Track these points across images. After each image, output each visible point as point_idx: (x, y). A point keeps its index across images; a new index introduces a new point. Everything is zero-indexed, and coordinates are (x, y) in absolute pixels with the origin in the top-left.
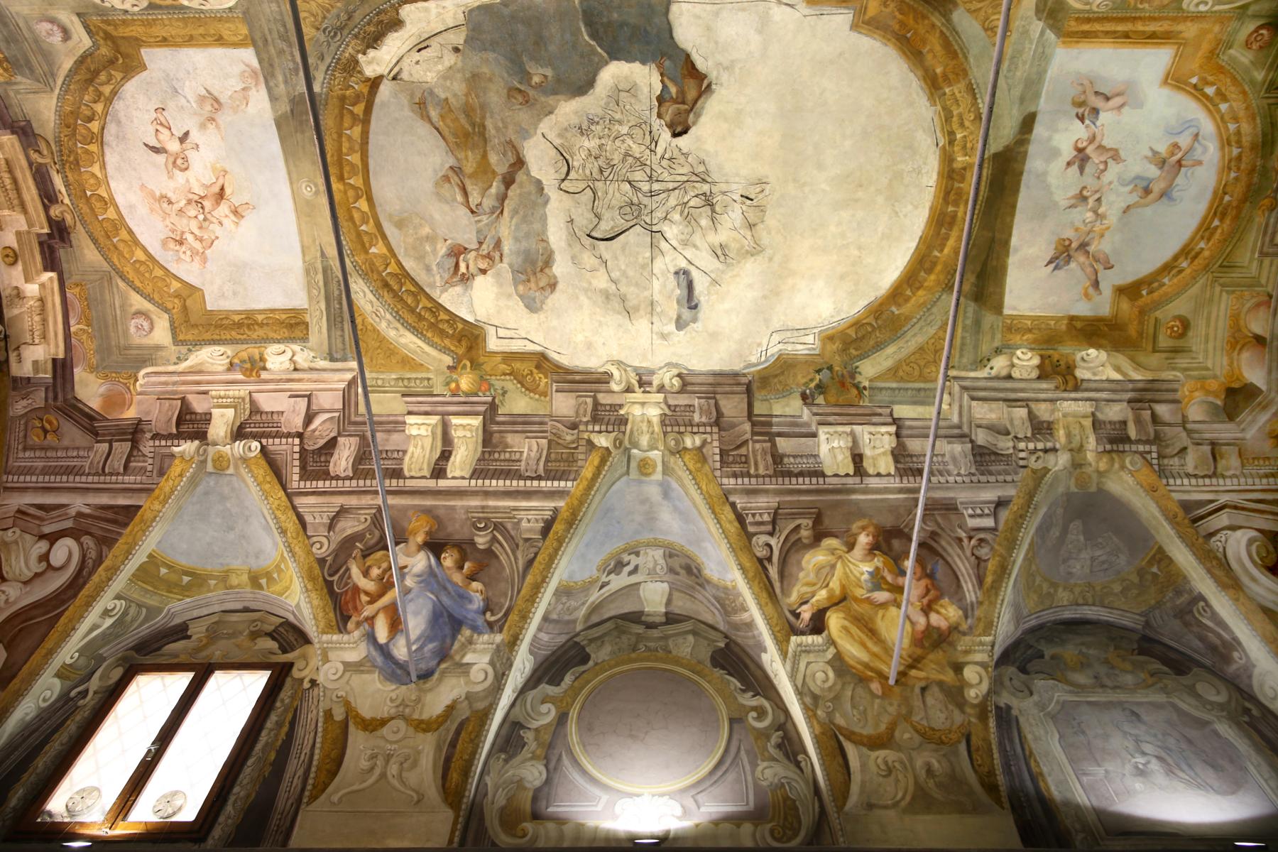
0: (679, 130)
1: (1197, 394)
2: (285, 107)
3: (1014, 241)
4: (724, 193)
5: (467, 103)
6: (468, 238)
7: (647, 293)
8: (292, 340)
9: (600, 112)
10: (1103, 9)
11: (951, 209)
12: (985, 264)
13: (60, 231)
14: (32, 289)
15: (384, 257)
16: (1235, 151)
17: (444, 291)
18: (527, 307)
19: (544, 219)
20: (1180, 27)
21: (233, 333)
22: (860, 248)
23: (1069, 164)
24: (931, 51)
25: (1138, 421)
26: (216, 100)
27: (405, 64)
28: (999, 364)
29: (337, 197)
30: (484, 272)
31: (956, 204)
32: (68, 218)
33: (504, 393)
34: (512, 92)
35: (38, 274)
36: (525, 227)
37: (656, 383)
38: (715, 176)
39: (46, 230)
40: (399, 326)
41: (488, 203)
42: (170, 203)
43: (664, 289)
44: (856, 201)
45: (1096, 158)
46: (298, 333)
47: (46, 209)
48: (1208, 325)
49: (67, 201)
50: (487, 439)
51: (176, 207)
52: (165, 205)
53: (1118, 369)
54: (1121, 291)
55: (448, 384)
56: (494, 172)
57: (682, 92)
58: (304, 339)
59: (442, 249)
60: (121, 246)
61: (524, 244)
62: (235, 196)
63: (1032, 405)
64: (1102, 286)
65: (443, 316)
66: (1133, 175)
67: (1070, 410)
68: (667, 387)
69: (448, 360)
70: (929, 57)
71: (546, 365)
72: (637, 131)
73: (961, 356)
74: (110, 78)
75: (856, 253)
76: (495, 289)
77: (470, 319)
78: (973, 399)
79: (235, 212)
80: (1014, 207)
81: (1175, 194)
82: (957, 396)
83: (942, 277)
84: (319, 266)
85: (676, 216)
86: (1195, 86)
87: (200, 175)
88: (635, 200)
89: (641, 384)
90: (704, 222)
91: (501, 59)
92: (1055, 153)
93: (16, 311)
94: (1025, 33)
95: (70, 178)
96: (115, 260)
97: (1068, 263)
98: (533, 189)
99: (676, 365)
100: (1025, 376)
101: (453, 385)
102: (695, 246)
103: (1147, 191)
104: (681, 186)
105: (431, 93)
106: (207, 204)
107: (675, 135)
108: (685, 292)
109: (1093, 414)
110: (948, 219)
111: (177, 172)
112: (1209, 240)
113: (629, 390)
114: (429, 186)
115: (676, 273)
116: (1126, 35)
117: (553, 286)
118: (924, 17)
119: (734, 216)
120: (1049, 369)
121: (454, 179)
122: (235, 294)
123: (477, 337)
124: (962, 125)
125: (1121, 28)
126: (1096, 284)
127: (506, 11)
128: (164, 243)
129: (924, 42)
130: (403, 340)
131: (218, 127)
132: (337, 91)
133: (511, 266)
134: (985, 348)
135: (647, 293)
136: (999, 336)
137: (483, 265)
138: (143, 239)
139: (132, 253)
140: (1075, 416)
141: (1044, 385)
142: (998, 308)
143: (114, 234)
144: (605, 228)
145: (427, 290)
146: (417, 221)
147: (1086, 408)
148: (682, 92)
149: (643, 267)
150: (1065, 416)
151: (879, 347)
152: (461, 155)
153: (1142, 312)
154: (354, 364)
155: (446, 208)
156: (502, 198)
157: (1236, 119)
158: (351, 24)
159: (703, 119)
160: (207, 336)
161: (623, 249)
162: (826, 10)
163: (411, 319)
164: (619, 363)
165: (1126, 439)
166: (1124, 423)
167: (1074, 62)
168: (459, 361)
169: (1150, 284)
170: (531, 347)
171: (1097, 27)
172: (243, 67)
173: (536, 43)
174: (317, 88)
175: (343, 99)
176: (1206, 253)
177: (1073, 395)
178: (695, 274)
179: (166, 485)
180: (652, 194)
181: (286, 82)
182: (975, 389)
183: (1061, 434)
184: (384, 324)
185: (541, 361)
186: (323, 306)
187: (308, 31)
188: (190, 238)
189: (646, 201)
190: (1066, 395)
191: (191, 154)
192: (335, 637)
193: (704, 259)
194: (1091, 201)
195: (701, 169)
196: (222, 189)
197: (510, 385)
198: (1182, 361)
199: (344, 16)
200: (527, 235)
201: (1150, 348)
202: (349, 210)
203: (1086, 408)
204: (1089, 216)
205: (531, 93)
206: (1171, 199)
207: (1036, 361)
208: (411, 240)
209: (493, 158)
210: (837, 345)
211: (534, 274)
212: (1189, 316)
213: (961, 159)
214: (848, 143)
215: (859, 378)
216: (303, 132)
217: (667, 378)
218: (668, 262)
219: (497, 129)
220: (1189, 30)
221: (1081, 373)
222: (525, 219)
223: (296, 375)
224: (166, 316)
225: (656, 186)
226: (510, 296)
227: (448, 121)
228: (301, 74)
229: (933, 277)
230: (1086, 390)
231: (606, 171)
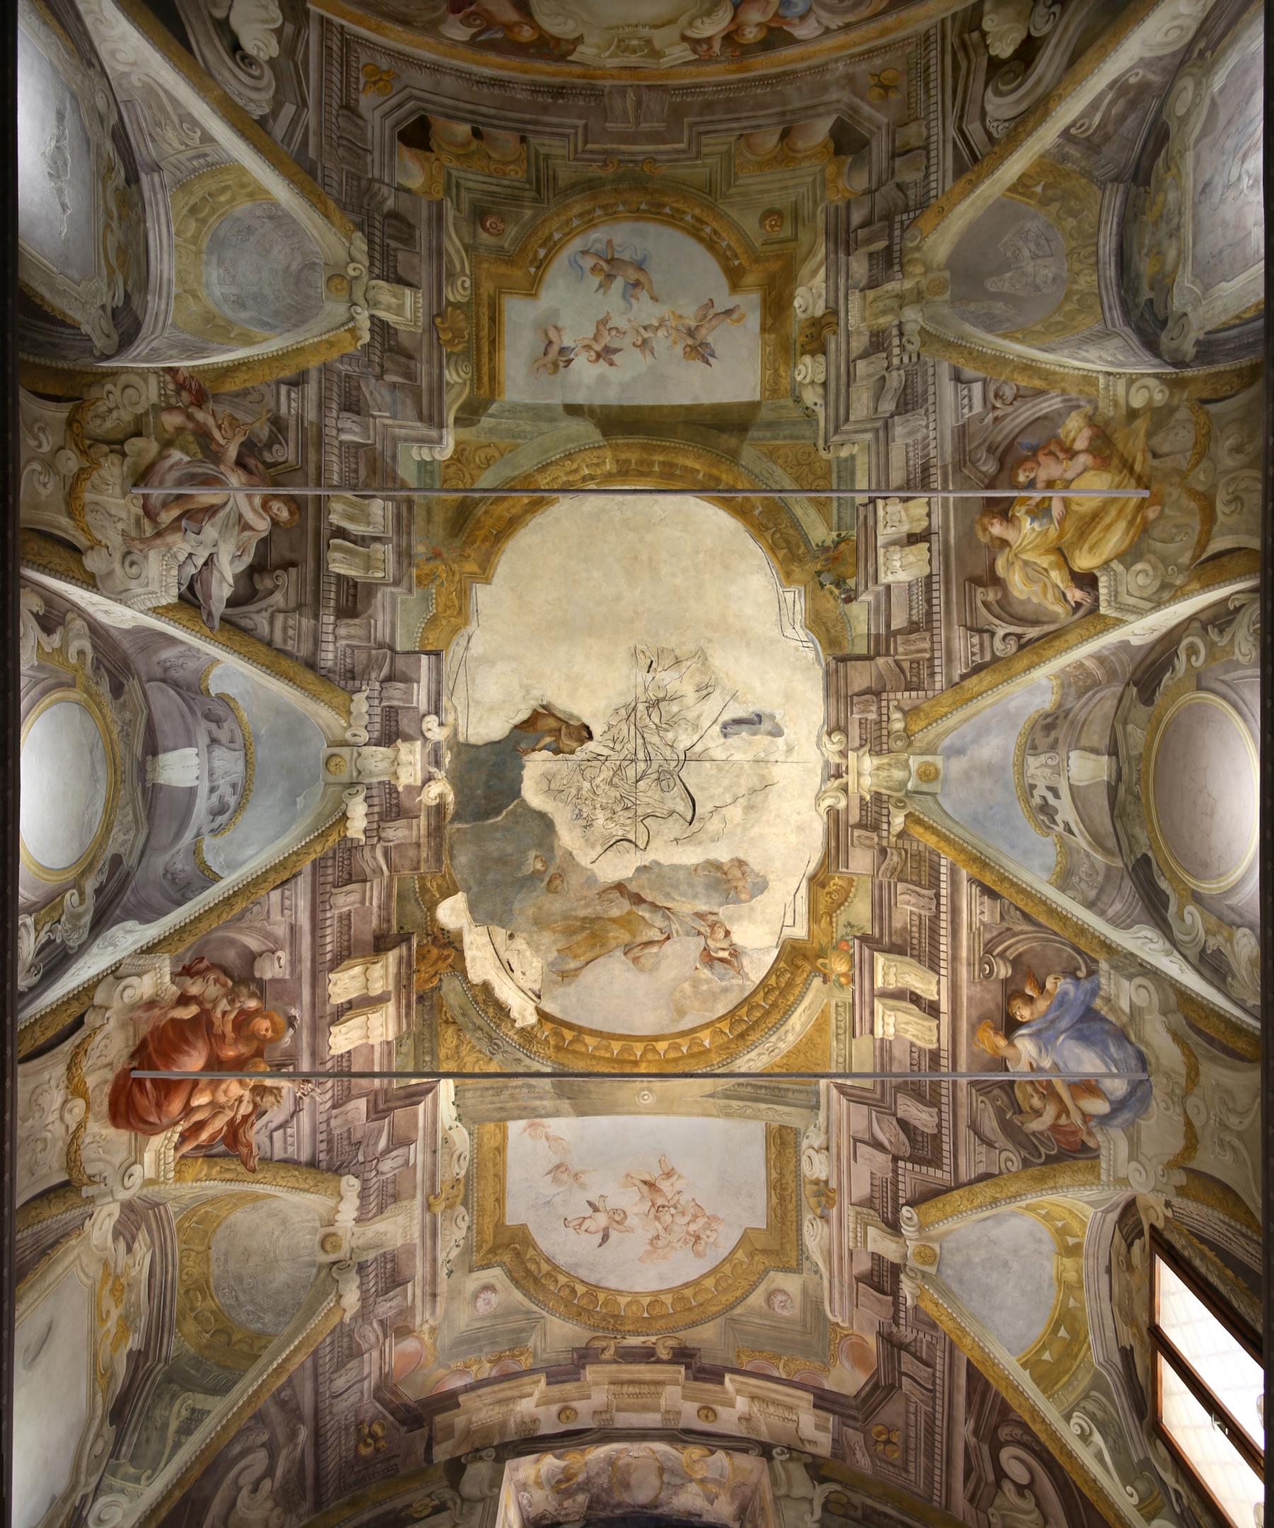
0: (585, 733)
1: (840, 186)
2: (565, 1104)
3: (687, 401)
4: (646, 689)
5: (562, 932)
6: (694, 946)
7: (746, 766)
8: (797, 1146)
9: (570, 808)
10: (469, 369)
11: (656, 468)
12: (710, 427)
13: (683, 1355)
15: (714, 1034)
16: (599, 212)
17: (746, 976)
18: (762, 892)
19: (675, 868)
20: (485, 297)
21: (790, 1207)
22: (697, 552)
23: (611, 364)
24: (508, 510)
25: (869, 241)
26: (558, 1167)
27: (527, 985)
28: (811, 397)
29: (654, 1070)
30: (727, 933)
31: (651, 464)
32: (670, 1343)
33: (850, 925)
34: (551, 888)
35: (726, 1392)
36: (683, 887)
37: (836, 759)
38: (630, 698)
39: (683, 1369)
40: (783, 1029)
41: (659, 921)
42: (657, 1237)
43: (742, 749)
44: (651, 560)
45: (606, 340)
46: (790, 1138)
47: (659, 1361)
48: (769, 191)
49: (653, 1339)
50: (898, 949)
51: (662, 1232)
52: (660, 1243)
53: (814, 273)
54: (735, 286)
55: (841, 986)
56: (629, 913)
57: (550, 732)
58: (796, 1132)
59: (705, 973)
60: (700, 1299)
61: (700, 889)
62: (654, 1174)
63: (853, 355)
64: (729, 306)
65: (773, 981)
66: (621, 302)
67: (856, 316)
68: (841, 747)
69: (817, 982)
70: (513, 511)
71: (821, 877)
72: (588, 773)
73: (803, 437)
74: (532, 1260)
75: (701, 556)
76: (746, 923)
77: (775, 953)
78: (847, 420)
79: (669, 1175)
80: (653, 408)
81: (639, 257)
82: (845, 437)
83: (724, 467)
84: (723, 1102)
85: (670, 736)
86: (538, 268)
87: (632, 1202)
88: (655, 776)
89: (838, 776)
90: (675, 708)
91: (520, 896)
92: (602, 380)
93: (764, 1428)
94: (491, 431)
95: (630, 1328)
96: (715, 1309)
97: (707, 345)
98: (645, 877)
99: (819, 737)
100: (823, 368)
101: (843, 980)
102: (699, 717)
103: (637, 284)
104: (640, 731)
105: (552, 964)
106: (660, 1201)
107: (590, 737)
108: (744, 727)
109: (862, 290)
110: (667, 470)
111: (627, 1223)
112: (684, 212)
113: (845, 789)
114: (643, 978)
115: (725, 736)
116: (492, 342)
117: (741, 863)
118: (478, 521)
119: (669, 679)
120: (815, 345)
121: (636, 952)
122: (750, 1196)
123: (793, 948)
124: (576, 471)
125: (486, 350)
126: (728, 313)
127: (475, 889)
128: (699, 1255)
129: (500, 518)
130: (798, 1028)
131: (584, 1172)
132: (551, 1052)
133: (721, 905)
134: (796, 414)
135: (746, 766)
136: (782, 402)
137: (722, 934)
138: (694, 1276)
139: (707, 1290)
140: (864, 309)
141: (832, 346)
142: (754, 406)
143: (686, 1302)
144: (682, 807)
145: (746, 994)
146: (677, 995)
147: (855, 297)
148: (550, 732)
149: (720, 769)
150: (864, 320)
151: (796, 524)
152: (613, 943)
153: (757, 260)
154: (823, 1082)
155: (664, 964)
156: (654, 907)
157: (568, 222)
158: (486, 1028)
159: (575, 711)
160: (793, 1235)
161: (702, 789)
162: (472, 607)
163: (776, 1016)
164: (818, 798)
165: (889, 249)
166: (871, 255)
167: (518, 379)
168: (818, 970)
169: (728, 259)
170: (803, 891)
171: (485, 370)
172: (526, 1135)
173: (505, 863)
174: (549, 1070)
175: (558, 1048)
176: (697, 211)
177: (842, 315)
178: (726, 717)
180: (648, 760)
181: (541, 1098)
182: (837, 419)
183: (882, 321)
184: (781, 1045)
185: (817, 881)
186: (763, 1106)
187: (493, 1068)
188: (693, 1227)
189: (655, 766)
190: (842, 323)
191: (611, 1203)
193: (712, 708)
194: (646, 335)
195: (623, 712)
196: (645, 1182)
197: (842, 917)
198: (807, 207)
199: (479, 1034)
200: (691, 885)
201: (792, 244)
202: (667, 1061)
203: (855, 297)
204: (661, 333)
205: (552, 871)
206: (644, 260)
207: (807, 359)
208: (697, 1004)
209: (615, 912)
210: (795, 567)
211: (730, 881)
212: (760, 212)
213: (609, 466)
214: (595, 574)
215: (829, 543)
216: (590, 1092)
217: (833, 746)
218: (715, 744)
219: (587, 906)
220: (487, 288)
221: (819, 310)
222: (675, 887)
223: (834, 1150)
224: (772, 1273)
225: (641, 755)
226: (752, 909)
227: (580, 951)
228: (532, 1081)
229: (724, 477)
230: (837, 302)
231: (627, 804)
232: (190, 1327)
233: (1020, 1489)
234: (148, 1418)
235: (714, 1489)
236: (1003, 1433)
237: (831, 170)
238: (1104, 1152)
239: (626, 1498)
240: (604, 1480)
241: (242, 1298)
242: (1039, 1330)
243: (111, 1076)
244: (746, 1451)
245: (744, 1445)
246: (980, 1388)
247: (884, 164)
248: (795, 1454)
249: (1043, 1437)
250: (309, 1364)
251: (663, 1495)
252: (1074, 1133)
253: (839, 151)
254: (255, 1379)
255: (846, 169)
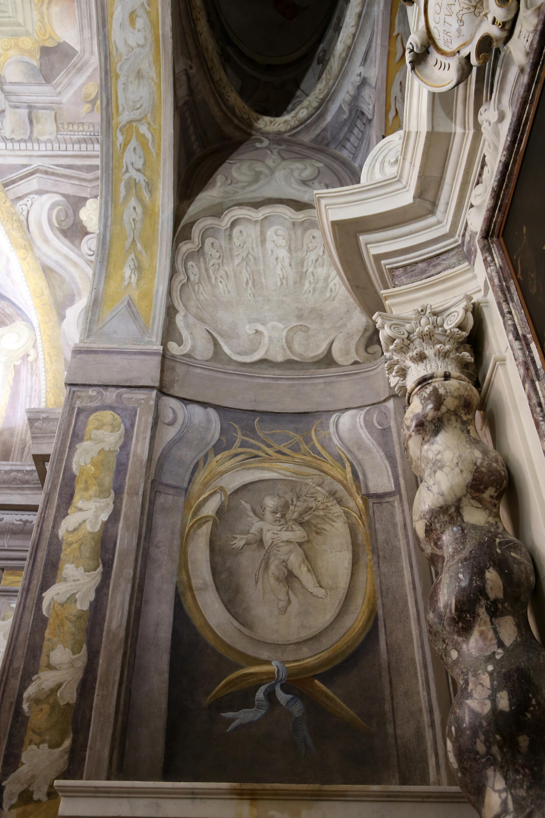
237: (27, 43)
247: (24, 99)
253: (45, 51)
255: (26, 58)
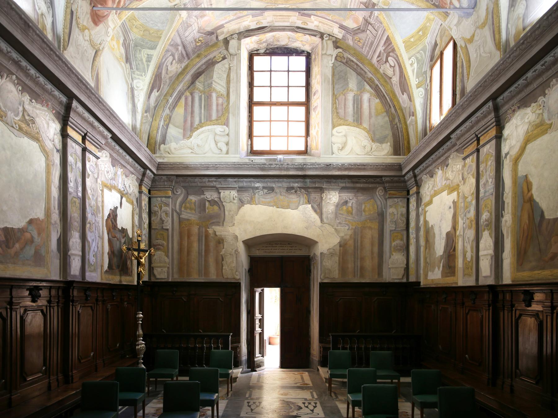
14: (316, 23)
179: (385, 24)
192: (448, 19)
232: (135, 30)
233: (391, 66)
234: (136, 57)
235: (305, 43)
236: (391, 54)
238: (450, 16)
239: (278, 43)
240: (272, 40)
241: (148, 20)
242: (414, 31)
243: (89, 16)
244: (315, 36)
245: (315, 33)
246: (389, 42)
248: (331, 37)
249: (401, 61)
250: (177, 34)
251: (289, 43)
252: (445, 4)
254: (162, 44)
